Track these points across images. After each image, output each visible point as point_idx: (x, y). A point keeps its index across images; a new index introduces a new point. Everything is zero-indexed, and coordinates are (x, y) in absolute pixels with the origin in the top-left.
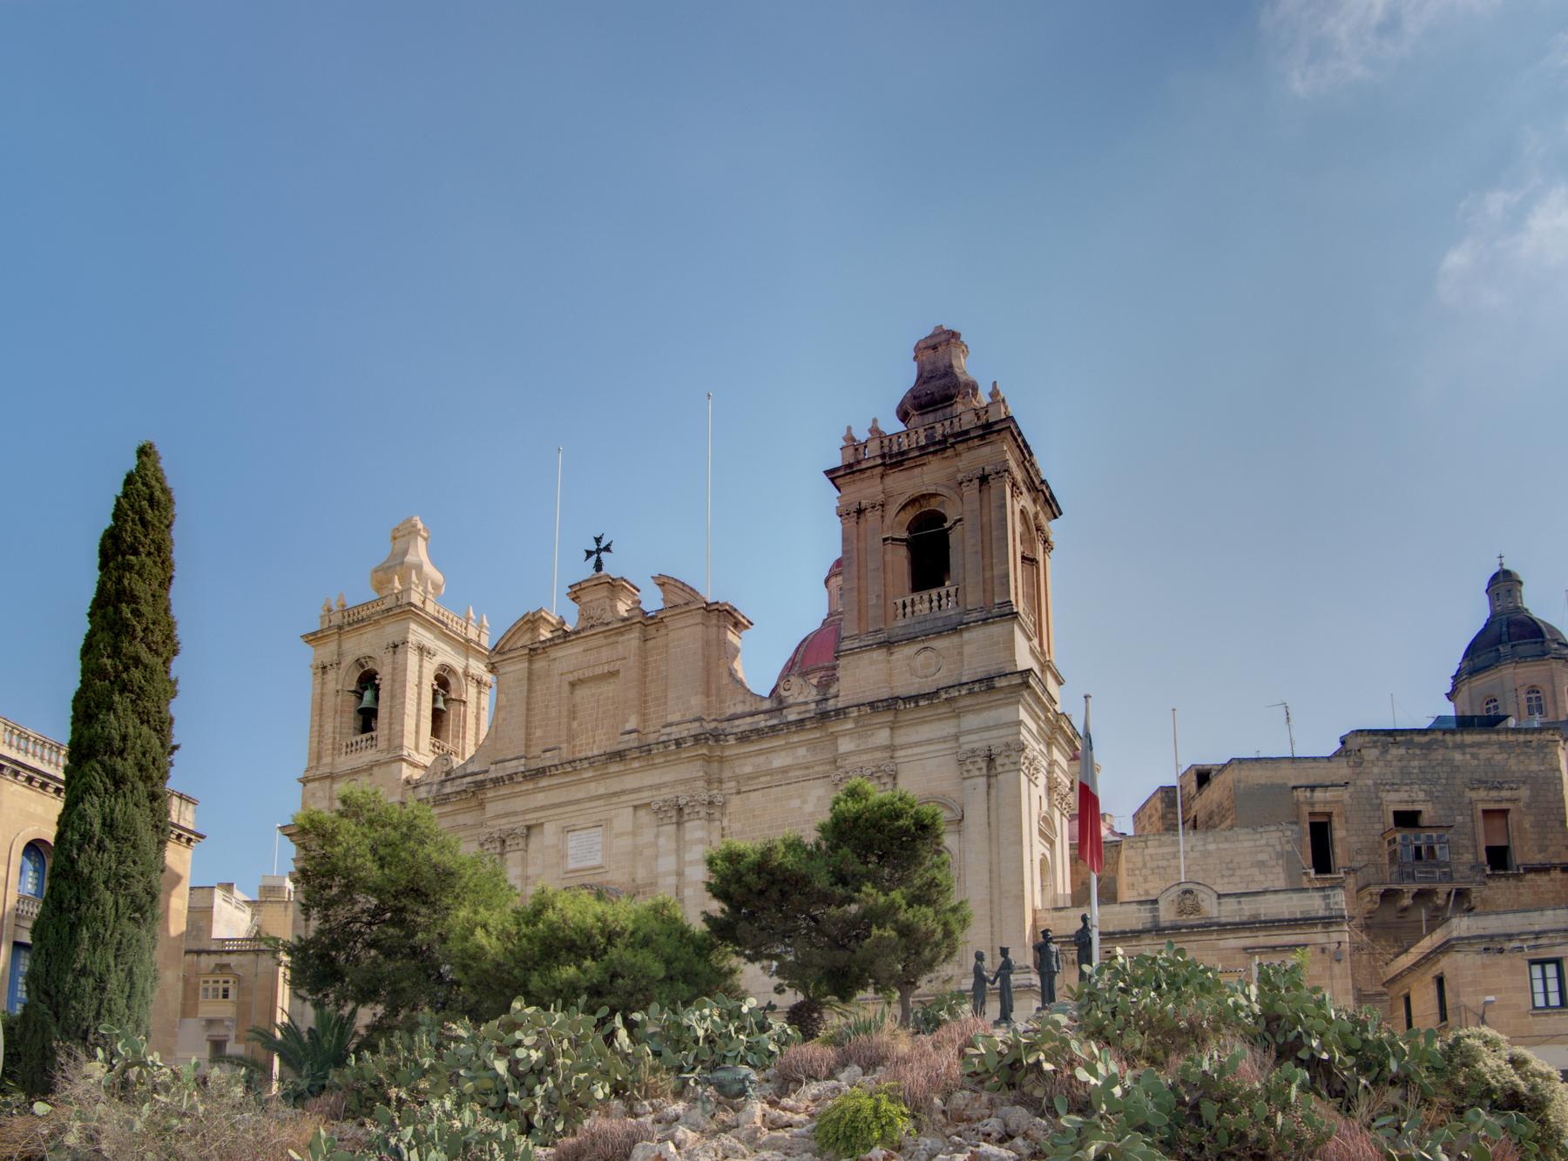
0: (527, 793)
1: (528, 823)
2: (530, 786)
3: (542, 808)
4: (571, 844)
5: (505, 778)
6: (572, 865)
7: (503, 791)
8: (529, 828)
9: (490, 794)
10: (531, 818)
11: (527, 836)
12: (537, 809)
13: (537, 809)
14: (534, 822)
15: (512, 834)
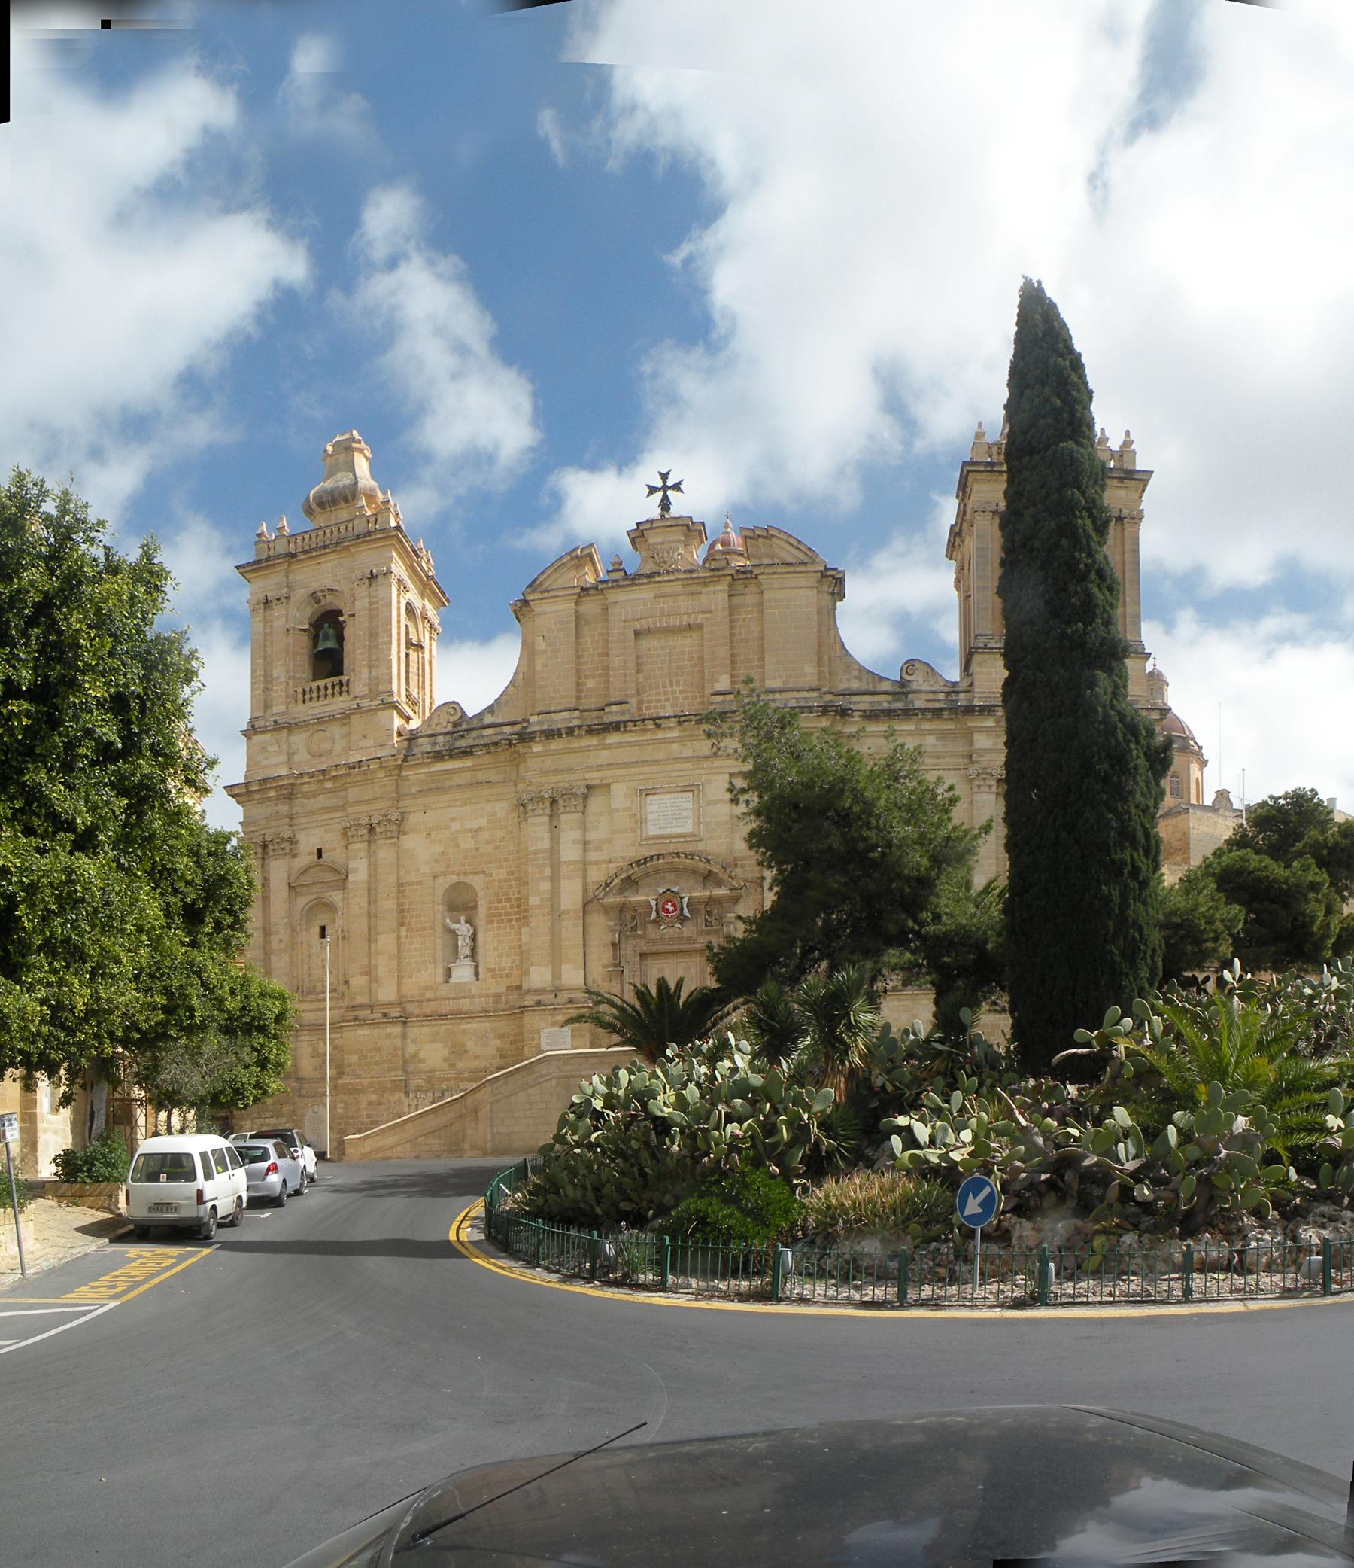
0: (588, 749)
1: (589, 782)
2: (593, 741)
3: (610, 766)
4: (650, 809)
5: (563, 731)
6: (652, 830)
7: (556, 745)
8: (588, 787)
9: (537, 748)
10: (594, 777)
11: (586, 797)
12: (600, 767)
13: (600, 767)
14: (597, 782)
15: (569, 794)
